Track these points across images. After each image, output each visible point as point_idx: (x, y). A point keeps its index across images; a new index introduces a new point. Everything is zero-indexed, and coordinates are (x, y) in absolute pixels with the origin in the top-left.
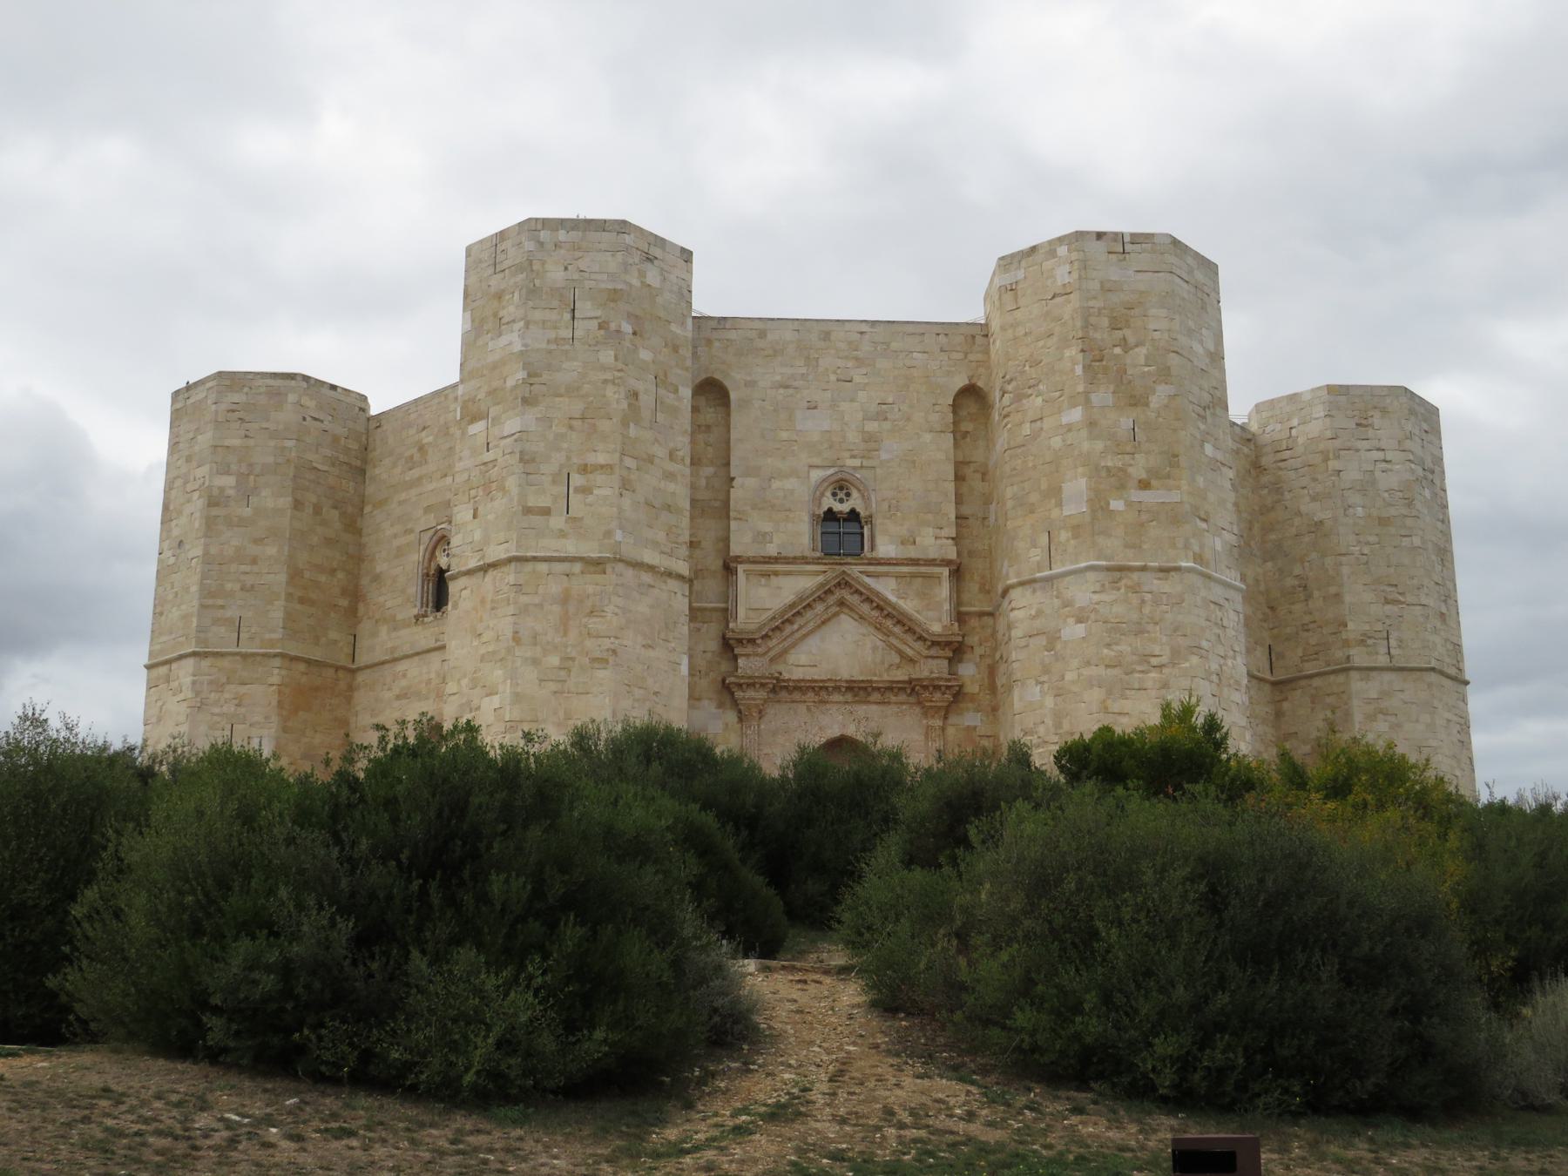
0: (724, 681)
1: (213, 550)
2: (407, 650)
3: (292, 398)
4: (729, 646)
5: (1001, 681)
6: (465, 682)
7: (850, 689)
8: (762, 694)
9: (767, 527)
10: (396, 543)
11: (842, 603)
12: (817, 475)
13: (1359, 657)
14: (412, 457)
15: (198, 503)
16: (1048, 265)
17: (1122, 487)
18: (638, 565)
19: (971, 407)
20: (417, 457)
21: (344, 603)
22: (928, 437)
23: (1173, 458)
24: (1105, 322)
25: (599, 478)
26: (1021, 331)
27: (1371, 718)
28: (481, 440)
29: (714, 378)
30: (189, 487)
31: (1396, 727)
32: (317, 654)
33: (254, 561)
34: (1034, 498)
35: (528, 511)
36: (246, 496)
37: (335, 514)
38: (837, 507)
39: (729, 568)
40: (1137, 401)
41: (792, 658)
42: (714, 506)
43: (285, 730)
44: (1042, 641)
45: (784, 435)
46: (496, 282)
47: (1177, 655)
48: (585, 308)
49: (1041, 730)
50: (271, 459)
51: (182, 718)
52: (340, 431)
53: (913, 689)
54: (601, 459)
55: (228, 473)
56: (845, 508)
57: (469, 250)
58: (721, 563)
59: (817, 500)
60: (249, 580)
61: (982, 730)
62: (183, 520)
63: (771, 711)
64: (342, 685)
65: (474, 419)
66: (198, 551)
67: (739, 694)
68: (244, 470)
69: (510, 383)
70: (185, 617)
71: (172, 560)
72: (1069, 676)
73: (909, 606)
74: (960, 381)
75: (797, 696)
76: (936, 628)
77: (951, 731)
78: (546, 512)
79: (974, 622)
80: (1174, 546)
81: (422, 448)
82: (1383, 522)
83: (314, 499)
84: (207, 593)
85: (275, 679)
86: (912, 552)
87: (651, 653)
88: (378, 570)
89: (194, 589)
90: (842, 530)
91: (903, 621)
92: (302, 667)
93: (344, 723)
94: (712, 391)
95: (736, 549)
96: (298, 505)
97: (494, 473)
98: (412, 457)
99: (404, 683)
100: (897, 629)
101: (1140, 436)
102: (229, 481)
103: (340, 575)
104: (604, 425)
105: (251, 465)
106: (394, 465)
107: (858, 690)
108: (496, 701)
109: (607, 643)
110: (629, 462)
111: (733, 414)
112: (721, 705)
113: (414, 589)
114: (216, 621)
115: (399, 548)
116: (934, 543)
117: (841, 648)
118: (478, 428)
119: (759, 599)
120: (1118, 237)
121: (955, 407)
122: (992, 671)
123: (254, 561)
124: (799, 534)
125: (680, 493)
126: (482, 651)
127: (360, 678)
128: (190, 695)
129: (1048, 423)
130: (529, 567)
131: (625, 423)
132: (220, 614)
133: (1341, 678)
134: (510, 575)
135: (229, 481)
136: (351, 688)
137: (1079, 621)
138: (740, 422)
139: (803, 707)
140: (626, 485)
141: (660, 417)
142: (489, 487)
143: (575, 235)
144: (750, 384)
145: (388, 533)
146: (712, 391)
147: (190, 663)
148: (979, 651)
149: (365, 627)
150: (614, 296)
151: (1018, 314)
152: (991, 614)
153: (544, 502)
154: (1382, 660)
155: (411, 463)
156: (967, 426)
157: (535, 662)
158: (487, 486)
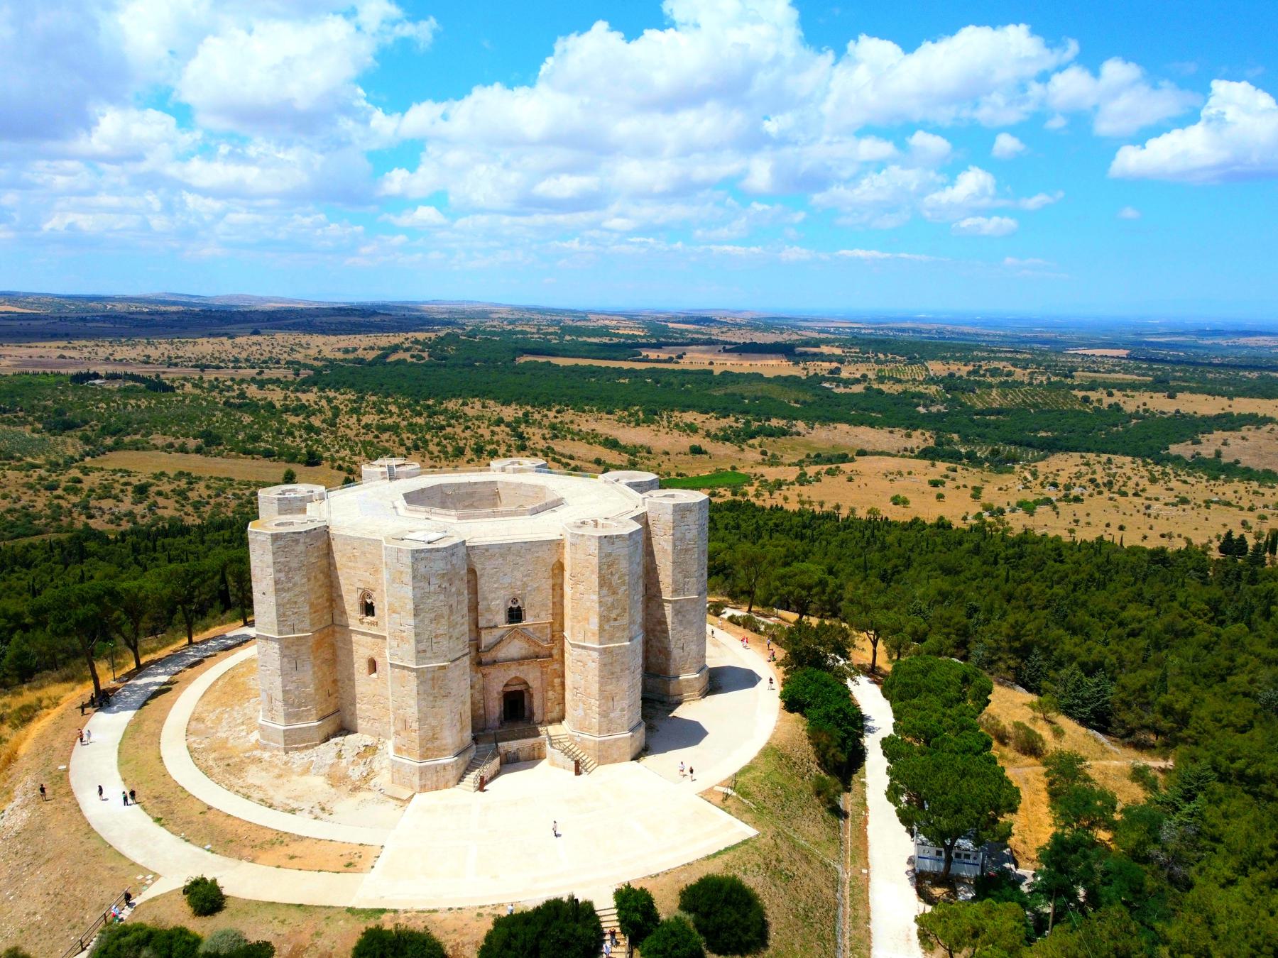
40: (614, 593)
48: (433, 580)
84: (279, 616)
90: (515, 615)
96: (309, 580)
107: (521, 660)
117: (515, 648)
120: (611, 537)
124: (501, 618)
135: (282, 575)
143: (428, 555)
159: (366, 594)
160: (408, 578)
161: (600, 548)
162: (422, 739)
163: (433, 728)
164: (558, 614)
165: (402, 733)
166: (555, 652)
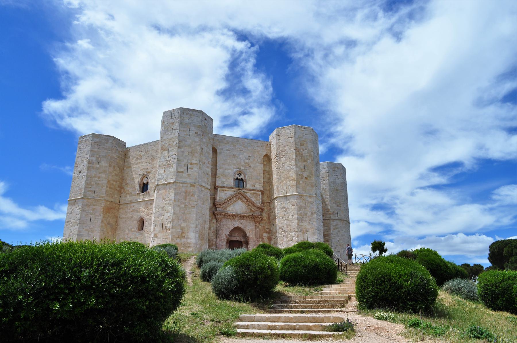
0: (213, 213)
1: (89, 174)
2: (134, 201)
3: (110, 141)
4: (215, 205)
5: (272, 217)
6: (160, 209)
7: (240, 216)
8: (221, 216)
9: (224, 180)
11: (239, 198)
12: (235, 170)
13: (332, 217)
15: (86, 163)
16: (287, 131)
17: (302, 178)
18: (201, 186)
19: (266, 159)
20: (139, 157)
21: (119, 189)
22: (258, 164)
23: (312, 174)
24: (299, 144)
25: (194, 166)
26: (281, 144)
27: (334, 229)
28: (167, 154)
29: (216, 147)
30: (83, 159)
31: (339, 231)
32: (112, 200)
33: (99, 178)
34: (283, 179)
35: (178, 172)
37: (118, 169)
38: (239, 177)
39: (215, 188)
40: (305, 161)
41: (228, 209)
42: (214, 175)
43: (104, 217)
45: (229, 161)
46: (172, 121)
47: (312, 214)
48: (192, 128)
49: (284, 229)
50: (104, 155)
51: (78, 213)
52: (120, 150)
53: (253, 217)
54: (195, 162)
55: (94, 157)
56: (240, 178)
57: (164, 113)
58: (213, 187)
59: (234, 175)
60: (98, 182)
61: (267, 227)
62: (81, 167)
63: (223, 220)
64: (117, 208)
65: (164, 150)
66: (85, 174)
67: (217, 216)
68: (98, 156)
69: (175, 143)
70: (80, 189)
72: (290, 217)
73: (253, 199)
74: (265, 153)
75: (229, 217)
76: (259, 205)
77: (260, 227)
78: (182, 172)
79: (265, 204)
80: (312, 191)
81: (141, 156)
82: (337, 190)
83: (114, 165)
84: (87, 184)
85: (103, 206)
86: (254, 188)
87: (204, 206)
89: (83, 183)
91: (252, 203)
92: (109, 203)
93: (117, 217)
94: (215, 151)
95: (217, 184)
96: (110, 166)
99: (133, 208)
100: (250, 204)
101: (306, 168)
102: (94, 159)
103: (118, 183)
104: (196, 155)
105: (99, 155)
107: (242, 217)
108: (169, 214)
109: (195, 203)
110: (201, 163)
111: (218, 156)
112: (212, 218)
113: (137, 187)
114: (89, 191)
116: (258, 186)
117: (238, 207)
118: (166, 153)
119: (222, 195)
121: (263, 158)
122: (269, 215)
123: (99, 178)
124: (231, 182)
125: (209, 171)
127: (121, 206)
128: (81, 207)
130: (178, 184)
131: (200, 155)
132: (90, 189)
133: (329, 221)
135: (94, 159)
136: (119, 209)
138: (219, 157)
139: (230, 220)
140: (200, 168)
141: (207, 154)
142: (169, 166)
144: (222, 149)
146: (215, 151)
147: (82, 200)
148: (266, 210)
149: (123, 195)
150: (199, 126)
151: (280, 141)
152: (269, 203)
153: (182, 170)
154: (337, 218)
155: (137, 159)
156: (265, 163)
157: (179, 206)
159: (145, 176)
160: (176, 126)
161: (295, 132)
162: (173, 236)
163: (183, 228)
164: (268, 181)
165: (159, 235)
166: (265, 215)
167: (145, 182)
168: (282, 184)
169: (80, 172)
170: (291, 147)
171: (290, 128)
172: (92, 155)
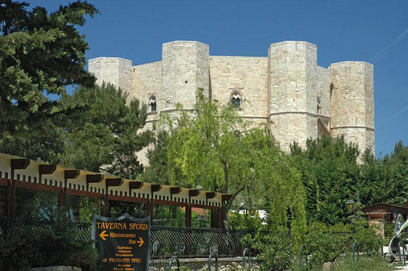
10: (220, 89)
14: (225, 70)
16: (357, 67)
34: (353, 111)
36: (203, 73)
40: (370, 97)
44: (354, 138)
46: (297, 53)
65: (291, 80)
69: (302, 76)
71: (183, 85)
81: (228, 69)
88: (214, 94)
97: (299, 93)
98: (225, 70)
106: (218, 70)
115: (221, 91)
118: (293, 83)
126: (297, 129)
129: (356, 97)
134: (305, 115)
135: (199, 69)
137: (362, 136)
145: (217, 86)
151: (351, 75)
155: (224, 71)
158: (297, 96)
167: (236, 97)
168: (352, 115)
169: (186, 82)
170: (361, 83)
171: (361, 65)
172: (198, 67)
